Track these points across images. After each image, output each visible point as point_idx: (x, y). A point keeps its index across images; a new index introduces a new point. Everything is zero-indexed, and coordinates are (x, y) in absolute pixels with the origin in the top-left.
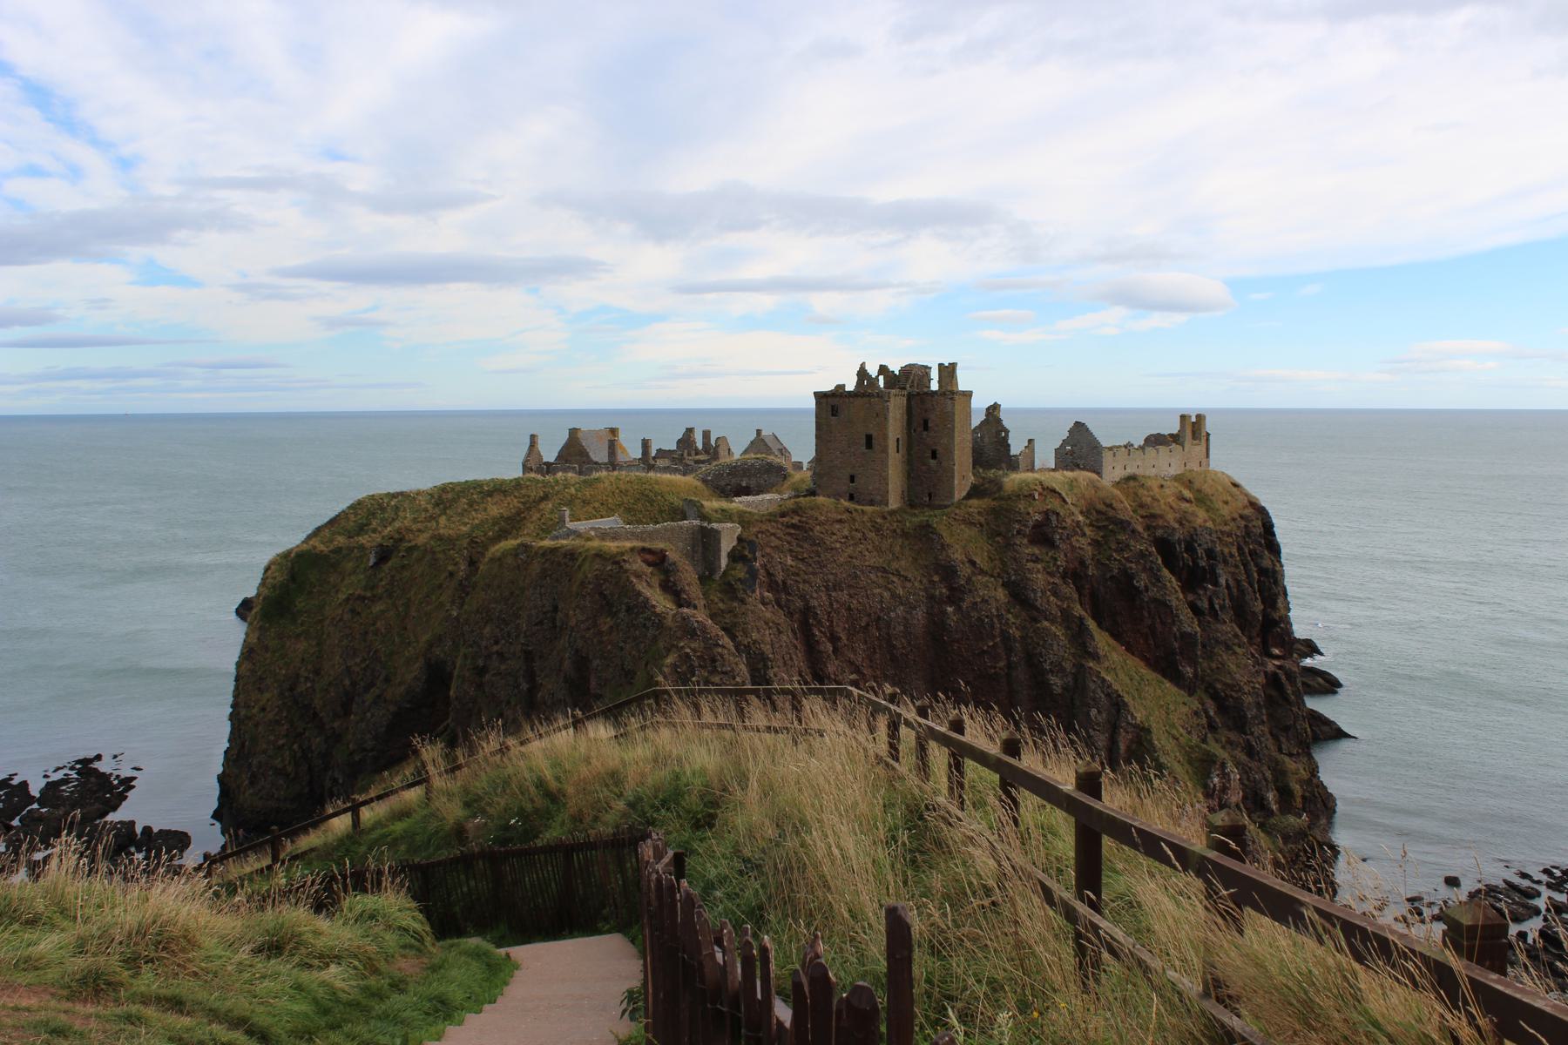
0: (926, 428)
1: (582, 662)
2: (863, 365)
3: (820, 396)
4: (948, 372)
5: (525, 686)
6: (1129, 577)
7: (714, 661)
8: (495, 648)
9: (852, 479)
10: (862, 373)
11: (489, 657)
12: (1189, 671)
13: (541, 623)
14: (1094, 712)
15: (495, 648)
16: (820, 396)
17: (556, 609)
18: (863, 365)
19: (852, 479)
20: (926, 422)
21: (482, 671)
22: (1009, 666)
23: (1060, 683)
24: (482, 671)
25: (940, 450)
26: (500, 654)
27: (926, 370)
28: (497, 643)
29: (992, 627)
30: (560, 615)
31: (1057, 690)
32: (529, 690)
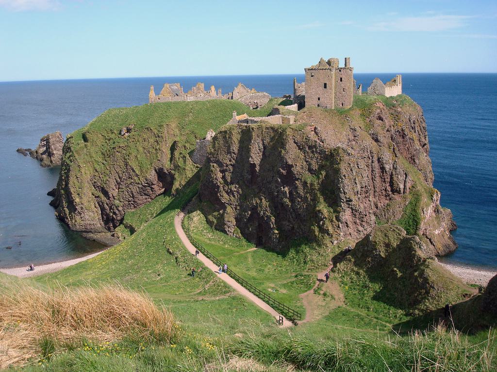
0: (341, 80)
6: (403, 130)
9: (319, 99)
12: (417, 161)
14: (399, 177)
19: (319, 99)
20: (341, 79)
22: (372, 162)
23: (388, 167)
25: (347, 88)
29: (367, 149)
31: (387, 170)
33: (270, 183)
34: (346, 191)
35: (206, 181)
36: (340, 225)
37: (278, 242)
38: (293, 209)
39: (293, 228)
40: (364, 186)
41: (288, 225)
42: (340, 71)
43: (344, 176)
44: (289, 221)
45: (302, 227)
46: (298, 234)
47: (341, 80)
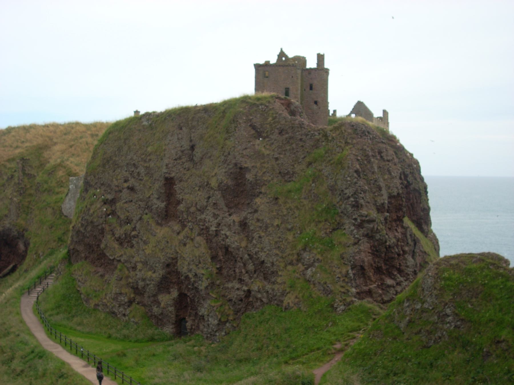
0: (311, 88)
1: (239, 172)
2: (281, 49)
3: (257, 67)
4: (321, 58)
5: (163, 205)
7: (380, 153)
8: (126, 185)
10: (282, 54)
11: (121, 191)
12: (425, 227)
13: (180, 158)
15: (126, 185)
16: (257, 67)
17: (193, 148)
18: (281, 49)
21: (113, 202)
24: (113, 202)
25: (319, 100)
26: (132, 189)
27: (301, 61)
28: (126, 181)
30: (198, 153)
32: (166, 207)
33: (201, 210)
34: (362, 201)
35: (82, 225)
36: (350, 271)
37: (218, 324)
38: (249, 255)
39: (249, 291)
40: (395, 194)
41: (238, 289)
42: (310, 73)
43: (357, 171)
44: (241, 281)
45: (268, 287)
46: (259, 303)
47: (311, 88)
